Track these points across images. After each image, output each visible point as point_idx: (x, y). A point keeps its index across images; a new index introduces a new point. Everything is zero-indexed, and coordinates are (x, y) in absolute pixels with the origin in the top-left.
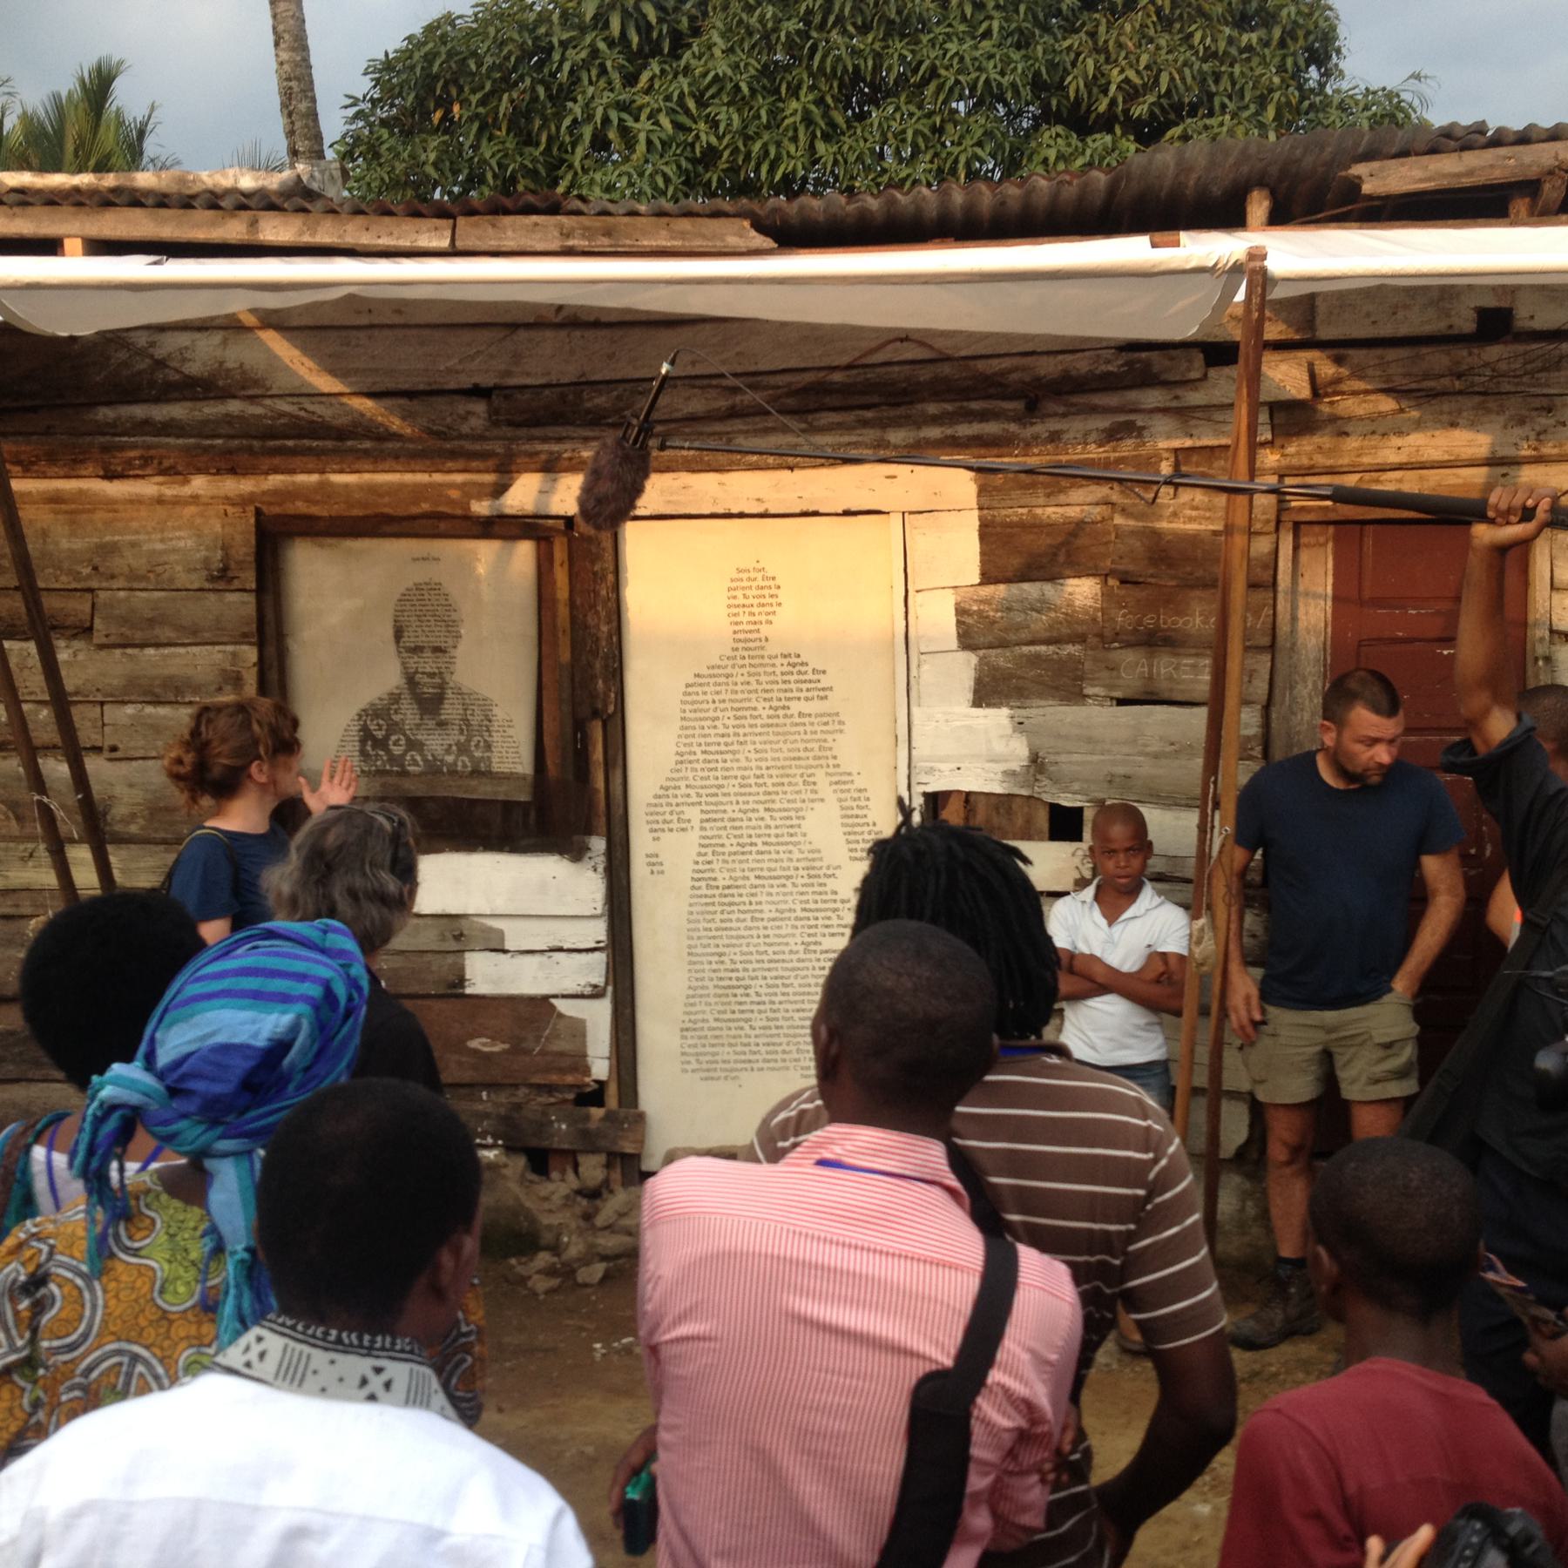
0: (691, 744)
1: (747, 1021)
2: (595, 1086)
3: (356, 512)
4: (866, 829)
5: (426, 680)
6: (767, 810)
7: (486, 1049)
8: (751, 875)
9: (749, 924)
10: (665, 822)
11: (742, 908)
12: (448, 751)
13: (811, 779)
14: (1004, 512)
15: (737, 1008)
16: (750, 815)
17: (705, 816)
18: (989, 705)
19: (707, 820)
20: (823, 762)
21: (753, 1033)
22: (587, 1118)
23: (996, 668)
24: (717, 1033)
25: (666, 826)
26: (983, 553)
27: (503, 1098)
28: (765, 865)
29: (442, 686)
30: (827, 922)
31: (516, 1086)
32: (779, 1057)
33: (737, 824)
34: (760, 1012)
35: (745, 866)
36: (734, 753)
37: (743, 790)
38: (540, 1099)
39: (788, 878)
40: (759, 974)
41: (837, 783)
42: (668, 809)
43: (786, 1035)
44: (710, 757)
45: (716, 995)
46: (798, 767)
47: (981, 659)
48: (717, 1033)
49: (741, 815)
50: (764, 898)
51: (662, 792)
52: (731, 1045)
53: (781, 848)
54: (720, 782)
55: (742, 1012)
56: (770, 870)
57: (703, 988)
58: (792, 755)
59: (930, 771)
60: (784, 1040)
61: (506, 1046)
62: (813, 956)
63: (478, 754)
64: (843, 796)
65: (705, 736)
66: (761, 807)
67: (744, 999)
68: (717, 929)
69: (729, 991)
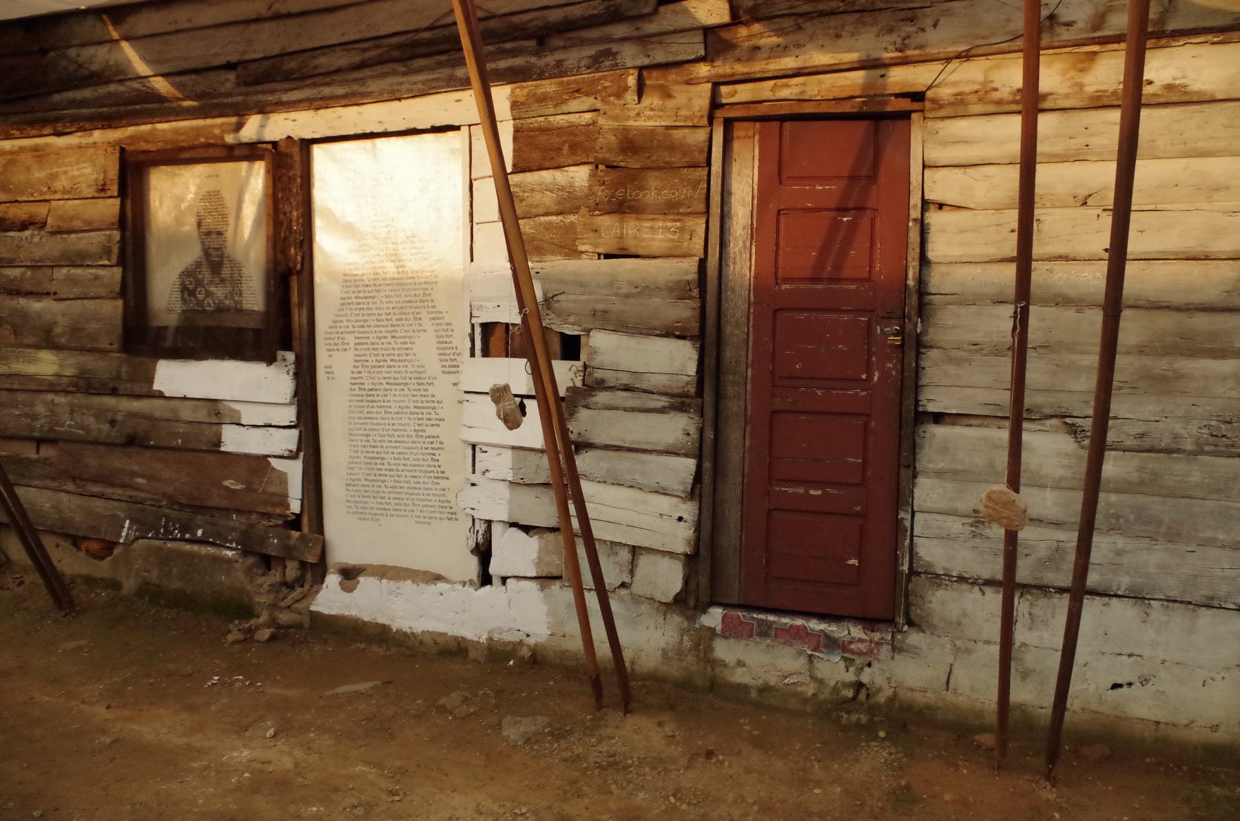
0: (349, 292)
1: (384, 481)
2: (294, 517)
3: (169, 146)
5: (214, 253)
6: (393, 337)
7: (233, 487)
8: (384, 382)
9: (384, 416)
10: (335, 344)
12: (226, 297)
13: (418, 316)
14: (529, 121)
16: (383, 340)
19: (359, 344)
20: (426, 304)
21: (387, 490)
22: (289, 537)
24: (366, 489)
25: (335, 347)
27: (243, 519)
29: (221, 256)
30: (429, 416)
31: (250, 512)
32: (402, 507)
34: (391, 476)
36: (373, 297)
37: (378, 323)
38: (264, 522)
40: (390, 450)
41: (434, 319)
43: (406, 493)
44: (360, 301)
48: (366, 489)
49: (378, 341)
51: (333, 324)
52: (374, 497)
54: (365, 318)
55: (380, 475)
56: (395, 378)
57: (357, 457)
58: (408, 299)
60: (406, 496)
61: (244, 486)
62: (420, 440)
63: (236, 298)
66: (389, 335)
67: (381, 467)
68: (365, 418)
69: (373, 461)
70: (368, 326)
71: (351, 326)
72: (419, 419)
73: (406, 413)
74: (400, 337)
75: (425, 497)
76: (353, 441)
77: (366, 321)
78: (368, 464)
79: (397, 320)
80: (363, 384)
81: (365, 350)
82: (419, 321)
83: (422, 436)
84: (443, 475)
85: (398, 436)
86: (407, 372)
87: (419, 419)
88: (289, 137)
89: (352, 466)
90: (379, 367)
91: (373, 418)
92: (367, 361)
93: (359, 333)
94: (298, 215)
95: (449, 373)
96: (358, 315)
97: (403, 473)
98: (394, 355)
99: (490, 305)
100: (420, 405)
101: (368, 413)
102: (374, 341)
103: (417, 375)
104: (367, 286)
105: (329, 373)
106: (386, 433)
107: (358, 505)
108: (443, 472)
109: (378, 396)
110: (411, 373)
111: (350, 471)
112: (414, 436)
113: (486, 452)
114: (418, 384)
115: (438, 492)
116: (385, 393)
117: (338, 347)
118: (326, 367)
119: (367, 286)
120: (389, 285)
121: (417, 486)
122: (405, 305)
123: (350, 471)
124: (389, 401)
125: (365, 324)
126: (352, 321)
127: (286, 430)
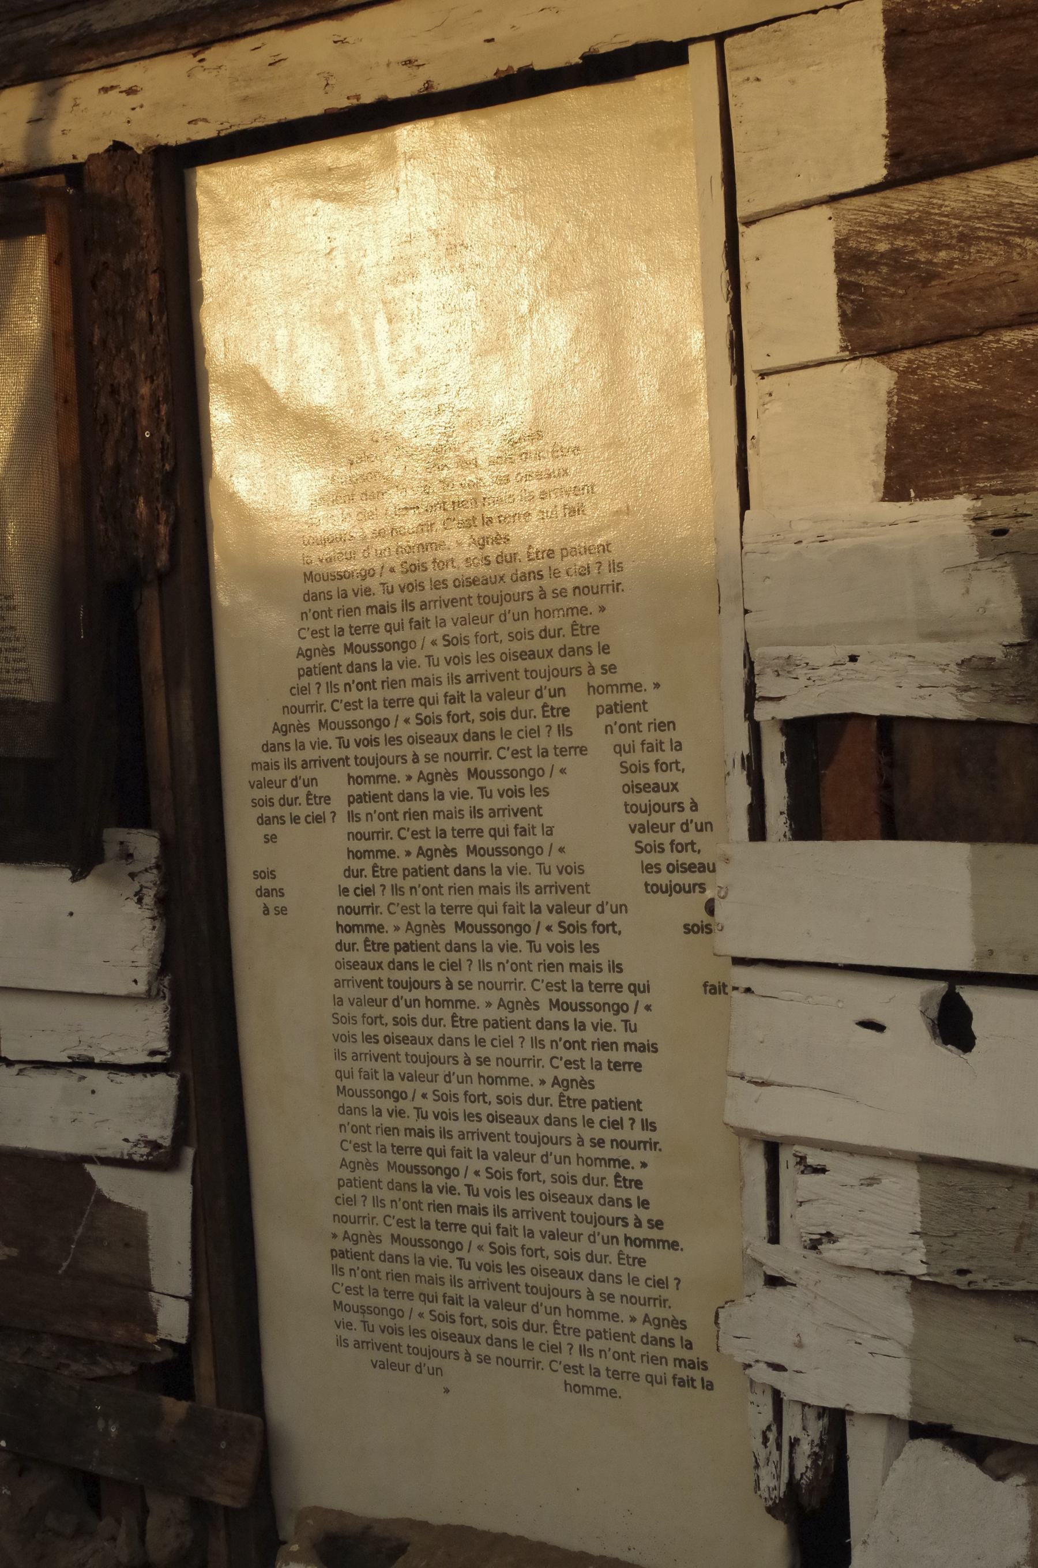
0: (324, 633)
1: (454, 1247)
2: (169, 1354)
4: (676, 817)
6: (472, 774)
8: (448, 921)
9: (451, 1032)
10: (285, 802)
11: (433, 994)
13: (557, 702)
15: (432, 1216)
16: (440, 785)
17: (357, 790)
18: (924, 494)
19: (361, 798)
20: (581, 660)
21: (465, 1275)
23: (938, 397)
24: (398, 1268)
25: (286, 811)
26: (893, 103)
28: (473, 900)
30: (605, 1037)
32: (519, 1335)
33: (416, 806)
34: (477, 1230)
35: (435, 900)
36: (403, 646)
37: (425, 730)
39: (521, 929)
40: (473, 1144)
41: (610, 710)
42: (289, 774)
43: (531, 1290)
45: (393, 1186)
46: (530, 674)
47: (904, 375)
48: (398, 1268)
49: (423, 787)
50: (475, 975)
51: (277, 738)
52: (425, 1297)
53: (503, 862)
54: (382, 713)
55: (444, 1226)
56: (484, 910)
57: (368, 1166)
58: (518, 646)
59: (786, 666)
60: (531, 1300)
62: (576, 1113)
64: (626, 739)
65: (349, 612)
67: (444, 1199)
68: (389, 1040)
70: (391, 741)
71: (334, 743)
72: (570, 1045)
73: (527, 1024)
74: (498, 774)
75: (597, 1305)
76: (351, 1111)
77: (381, 723)
78: (400, 1187)
79: (485, 716)
80: (380, 929)
81: (384, 817)
82: (561, 719)
83: (581, 1102)
84: (655, 1234)
85: (501, 1100)
86: (523, 888)
87: (570, 1045)
88: (118, 146)
89: (349, 1192)
90: (430, 872)
91: (414, 1040)
92: (391, 854)
93: (360, 761)
94: (153, 394)
95: (670, 890)
96: (357, 705)
97: (519, 1223)
98: (479, 832)
99: (819, 655)
100: (569, 996)
101: (397, 1022)
102: (412, 787)
103: (560, 899)
104: (383, 610)
105: (268, 893)
106: (455, 1087)
107: (371, 1319)
108: (658, 1224)
109: (429, 966)
110: (539, 890)
111: (345, 1210)
112: (554, 1100)
113: (822, 1170)
114: (564, 928)
115: (643, 1291)
116: (454, 957)
117: (295, 810)
118: (257, 875)
119: (383, 610)
120: (453, 601)
121: (569, 1266)
122: (509, 666)
123: (345, 1210)
124: (466, 985)
125: (380, 734)
126: (336, 725)
127: (139, 1077)
